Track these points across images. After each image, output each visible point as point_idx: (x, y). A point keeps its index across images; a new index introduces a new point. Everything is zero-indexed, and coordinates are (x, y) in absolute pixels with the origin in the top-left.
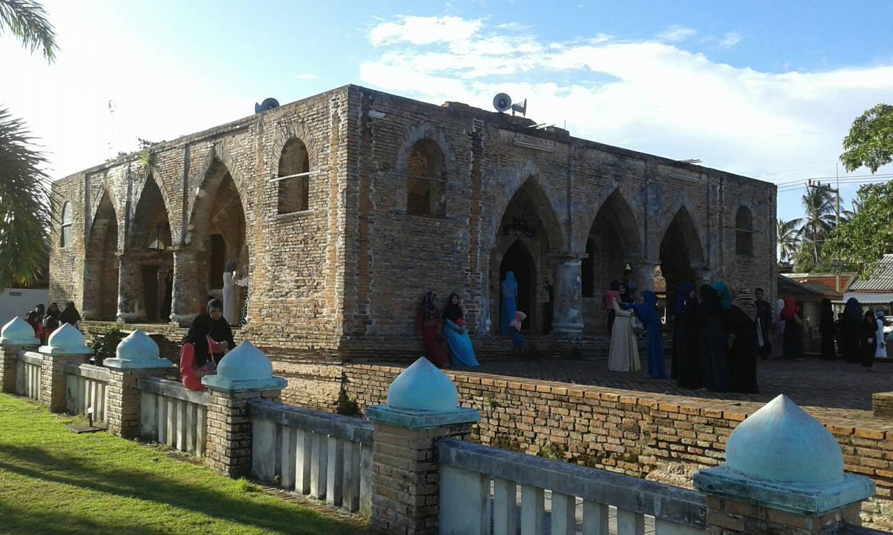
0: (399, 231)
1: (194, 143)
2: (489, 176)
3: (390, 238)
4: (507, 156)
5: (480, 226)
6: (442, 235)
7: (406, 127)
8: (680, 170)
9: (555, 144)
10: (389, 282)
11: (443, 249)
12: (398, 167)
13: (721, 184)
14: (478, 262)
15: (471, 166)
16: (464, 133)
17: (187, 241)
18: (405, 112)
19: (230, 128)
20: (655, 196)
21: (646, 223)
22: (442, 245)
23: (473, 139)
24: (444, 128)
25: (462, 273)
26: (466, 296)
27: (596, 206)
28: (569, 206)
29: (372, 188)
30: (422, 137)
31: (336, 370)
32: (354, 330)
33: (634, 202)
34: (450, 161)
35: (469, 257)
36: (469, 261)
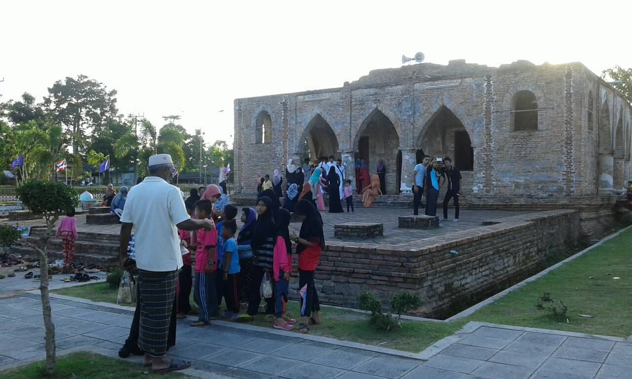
6: (270, 151)
8: (439, 82)
12: (252, 125)
13: (489, 81)
15: (283, 118)
20: (410, 106)
25: (280, 166)
27: (360, 121)
29: (242, 136)
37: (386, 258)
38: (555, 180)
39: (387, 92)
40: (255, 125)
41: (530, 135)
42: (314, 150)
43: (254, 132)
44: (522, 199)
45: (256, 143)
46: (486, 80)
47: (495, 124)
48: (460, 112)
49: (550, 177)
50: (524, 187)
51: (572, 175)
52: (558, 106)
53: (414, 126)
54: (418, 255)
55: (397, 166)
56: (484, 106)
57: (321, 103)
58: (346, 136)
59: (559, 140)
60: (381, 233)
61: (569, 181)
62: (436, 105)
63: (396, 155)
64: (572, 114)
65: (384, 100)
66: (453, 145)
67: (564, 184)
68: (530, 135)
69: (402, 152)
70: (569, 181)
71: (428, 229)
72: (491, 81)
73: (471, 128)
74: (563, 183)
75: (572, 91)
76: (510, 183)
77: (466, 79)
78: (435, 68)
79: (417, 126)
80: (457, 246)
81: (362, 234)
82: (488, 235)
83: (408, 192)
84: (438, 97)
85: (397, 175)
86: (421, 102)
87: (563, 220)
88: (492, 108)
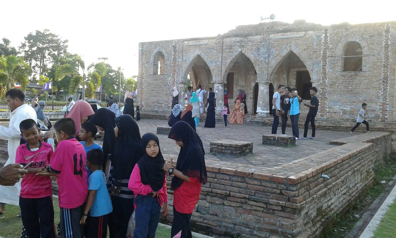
6: (163, 80)
8: (289, 33)
9: (209, 41)
12: (151, 62)
13: (326, 33)
15: (173, 57)
20: (266, 50)
22: (163, 83)
25: (170, 91)
26: (171, 99)
27: (229, 61)
30: (158, 51)
37: (264, 184)
38: (373, 109)
39: (249, 40)
40: (153, 61)
41: (356, 75)
42: (195, 81)
43: (152, 66)
44: (348, 123)
45: (153, 74)
46: (324, 33)
47: (329, 66)
48: (303, 56)
49: (370, 107)
50: (350, 114)
51: (387, 106)
52: (378, 53)
53: (268, 65)
54: (298, 182)
55: (253, 95)
56: (322, 52)
57: (201, 47)
58: (218, 71)
59: (378, 80)
60: (251, 151)
61: (384, 110)
62: (285, 51)
63: (253, 87)
64: (389, 60)
65: (247, 46)
66: (295, 81)
67: (381, 113)
68: (356, 75)
69: (259, 84)
70: (384, 110)
71: (288, 147)
72: (328, 34)
73: (311, 68)
74: (379, 112)
75: (389, 43)
76: (340, 110)
77: (309, 32)
78: (284, 25)
79: (271, 66)
80: (327, 170)
81: (235, 152)
82: (346, 157)
83: (262, 114)
84: (287, 45)
85: (253, 101)
86: (275, 48)
87: (383, 140)
88: (328, 53)
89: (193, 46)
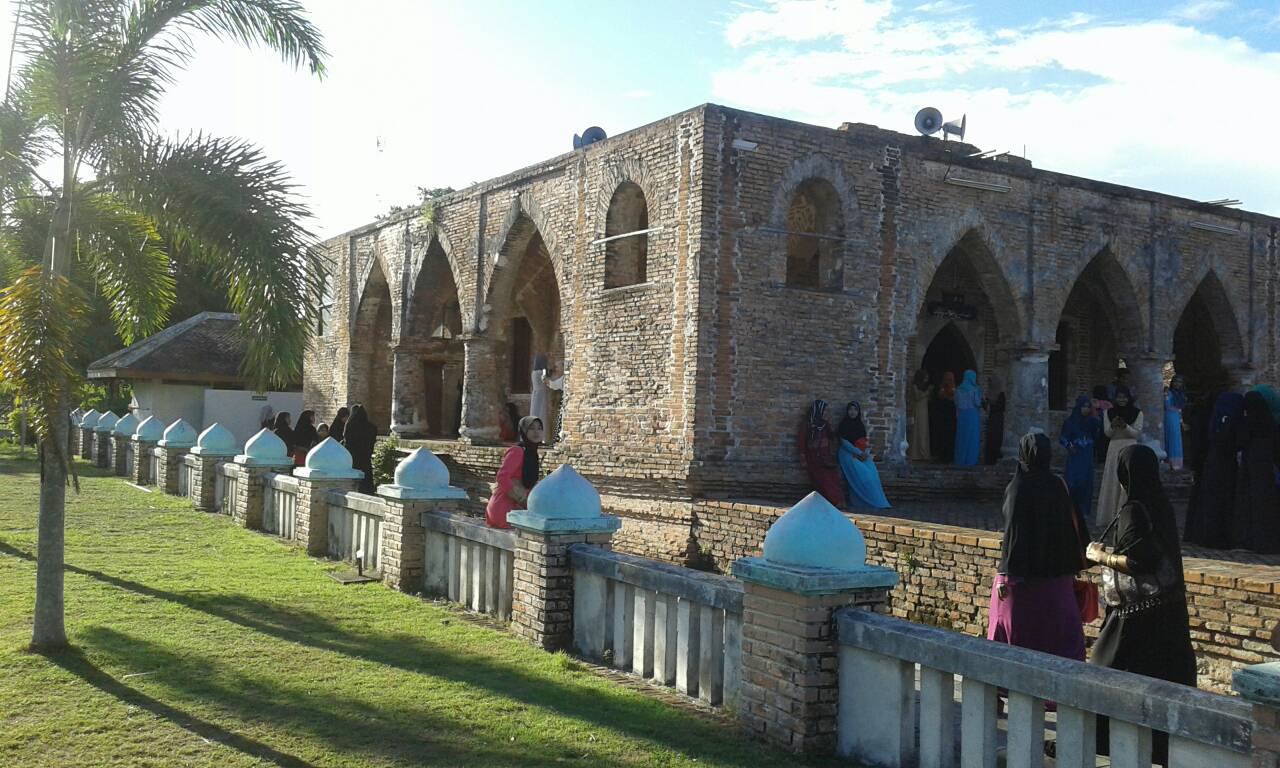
0: (774, 312)
1: (491, 192)
2: (909, 229)
3: (761, 321)
4: (935, 199)
5: (893, 304)
6: (836, 318)
7: (786, 161)
9: (1009, 181)
10: (758, 385)
11: (839, 339)
12: (774, 220)
14: (890, 357)
15: (881, 217)
16: (871, 167)
17: (483, 327)
18: (785, 141)
19: (540, 170)
20: (1167, 257)
21: (1151, 300)
22: (836, 332)
23: (884, 176)
24: (842, 161)
26: (871, 406)
27: (1073, 272)
28: (1030, 273)
29: (736, 250)
30: (809, 174)
31: (684, 509)
32: (710, 452)
33: (1132, 265)
34: (850, 210)
35: (876, 349)
36: (876, 355)
89: (955, 191)
